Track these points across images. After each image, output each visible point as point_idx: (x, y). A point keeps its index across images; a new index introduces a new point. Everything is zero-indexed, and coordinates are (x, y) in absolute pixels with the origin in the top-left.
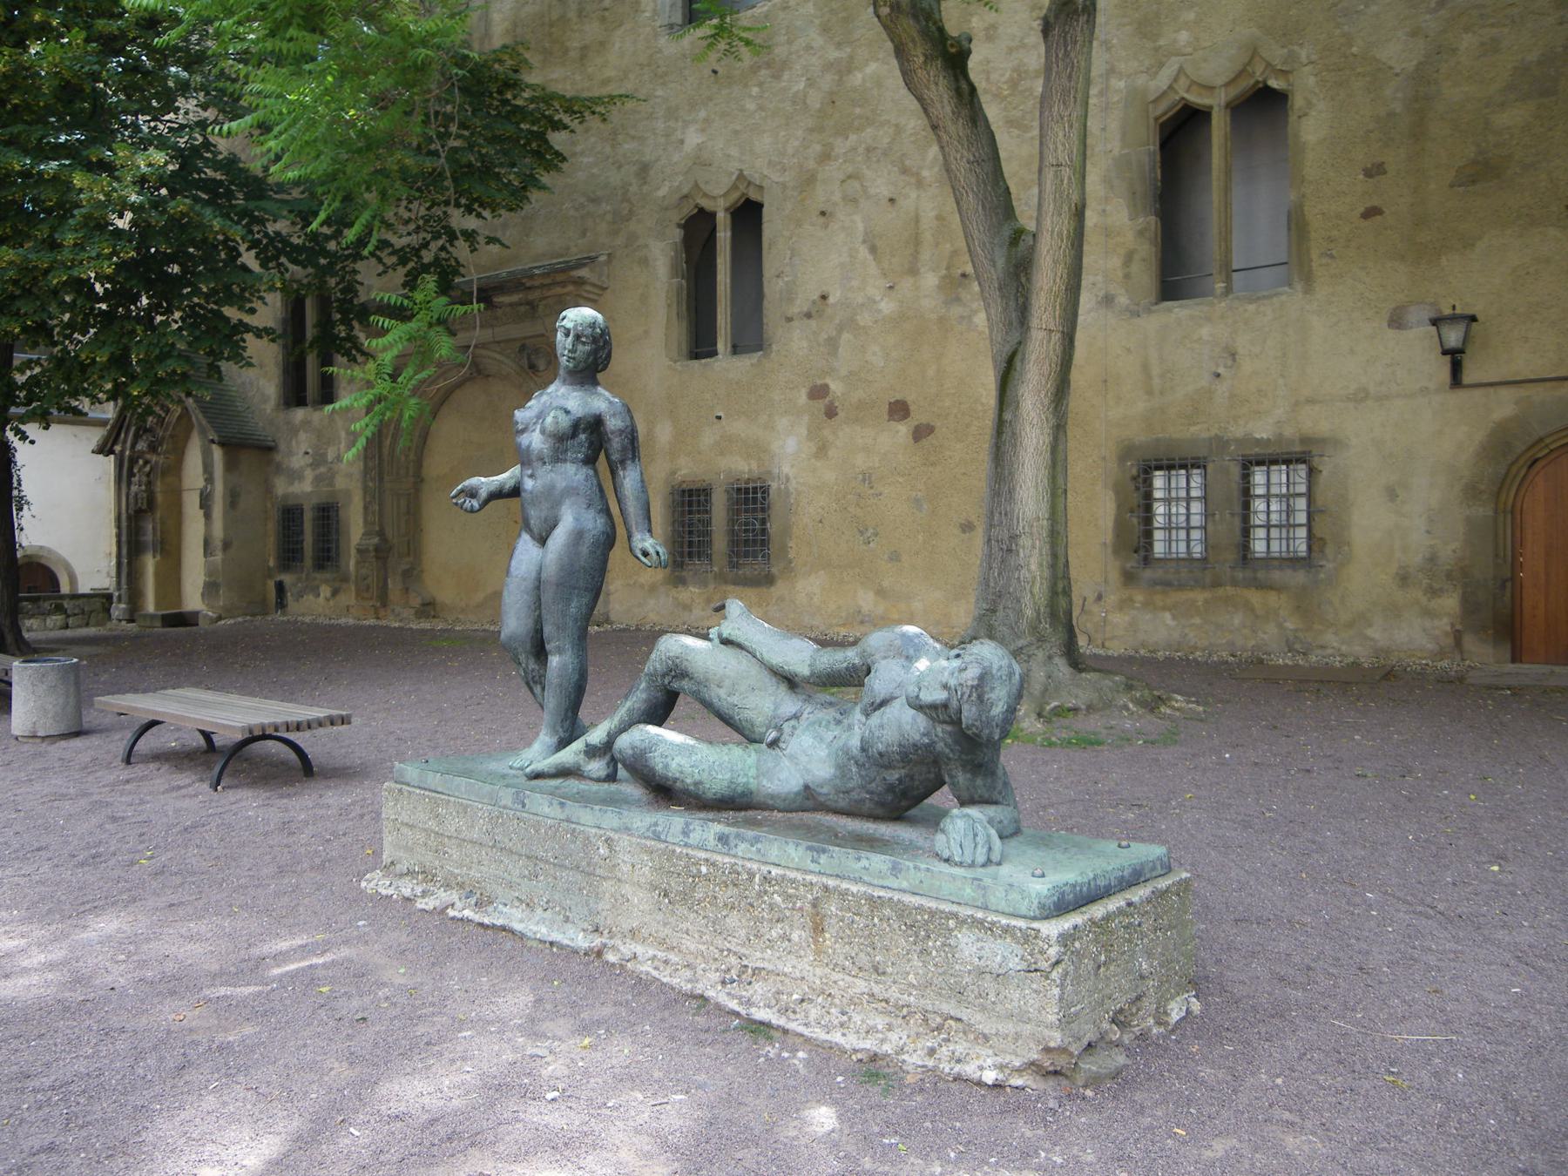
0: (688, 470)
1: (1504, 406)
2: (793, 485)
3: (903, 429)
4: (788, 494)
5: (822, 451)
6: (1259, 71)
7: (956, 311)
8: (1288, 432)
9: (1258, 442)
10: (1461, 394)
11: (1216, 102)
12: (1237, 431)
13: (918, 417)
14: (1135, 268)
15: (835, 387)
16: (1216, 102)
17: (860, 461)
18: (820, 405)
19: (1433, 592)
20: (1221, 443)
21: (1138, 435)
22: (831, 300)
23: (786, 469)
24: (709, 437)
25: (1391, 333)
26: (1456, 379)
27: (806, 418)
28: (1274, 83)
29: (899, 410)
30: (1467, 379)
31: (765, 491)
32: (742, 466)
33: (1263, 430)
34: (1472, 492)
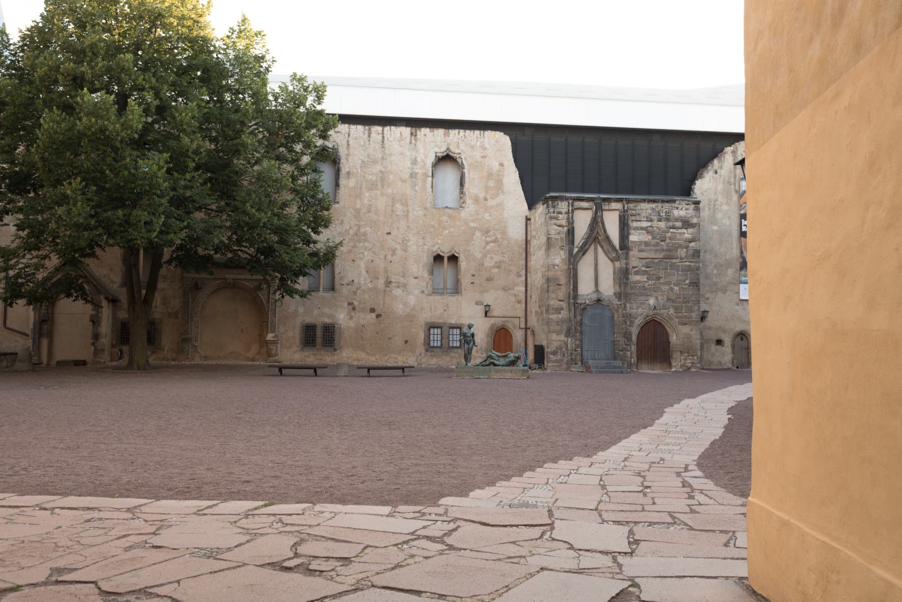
0: (309, 320)
1: (492, 321)
2: (342, 326)
3: (374, 315)
4: (341, 328)
5: (351, 318)
6: (453, 251)
7: (388, 289)
8: (458, 322)
9: (452, 324)
10: (486, 318)
11: (446, 256)
12: (449, 321)
13: (378, 312)
14: (429, 286)
15: (355, 303)
16: (446, 256)
17: (362, 322)
18: (351, 307)
19: (482, 354)
20: (445, 324)
21: (429, 321)
22: (355, 282)
23: (340, 322)
24: (316, 312)
25: (475, 306)
26: (486, 316)
27: (346, 310)
28: (456, 255)
29: (372, 310)
30: (488, 315)
31: (334, 327)
32: (328, 321)
33: (453, 322)
34: (488, 336)
